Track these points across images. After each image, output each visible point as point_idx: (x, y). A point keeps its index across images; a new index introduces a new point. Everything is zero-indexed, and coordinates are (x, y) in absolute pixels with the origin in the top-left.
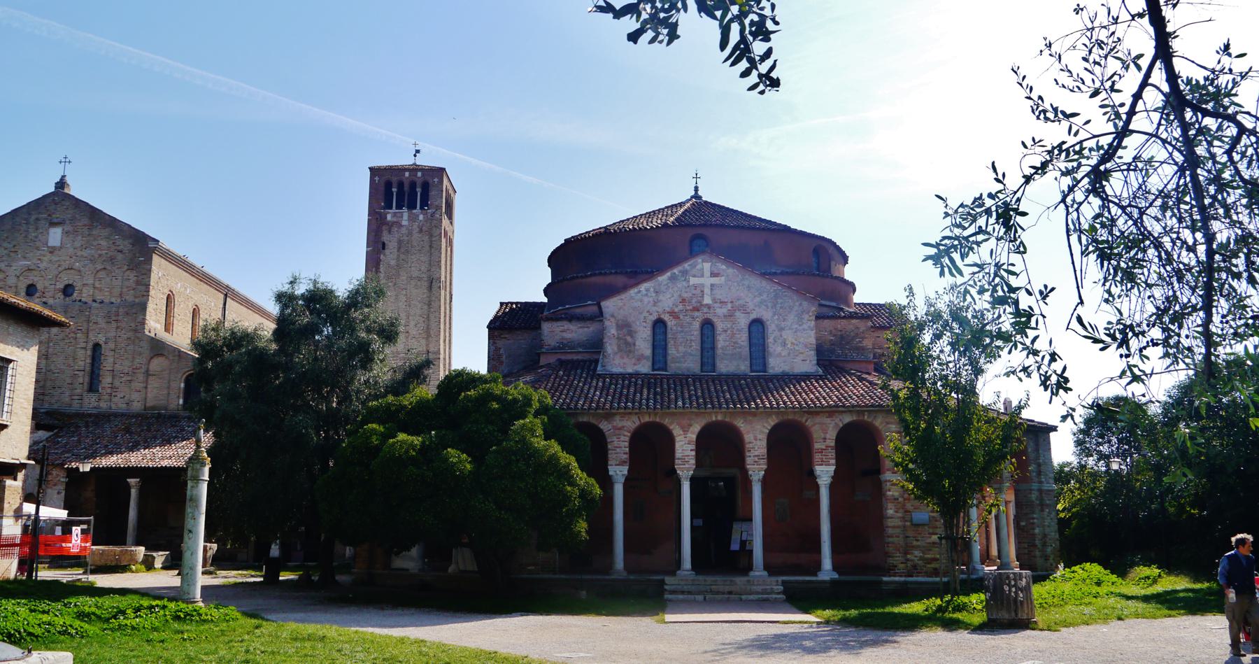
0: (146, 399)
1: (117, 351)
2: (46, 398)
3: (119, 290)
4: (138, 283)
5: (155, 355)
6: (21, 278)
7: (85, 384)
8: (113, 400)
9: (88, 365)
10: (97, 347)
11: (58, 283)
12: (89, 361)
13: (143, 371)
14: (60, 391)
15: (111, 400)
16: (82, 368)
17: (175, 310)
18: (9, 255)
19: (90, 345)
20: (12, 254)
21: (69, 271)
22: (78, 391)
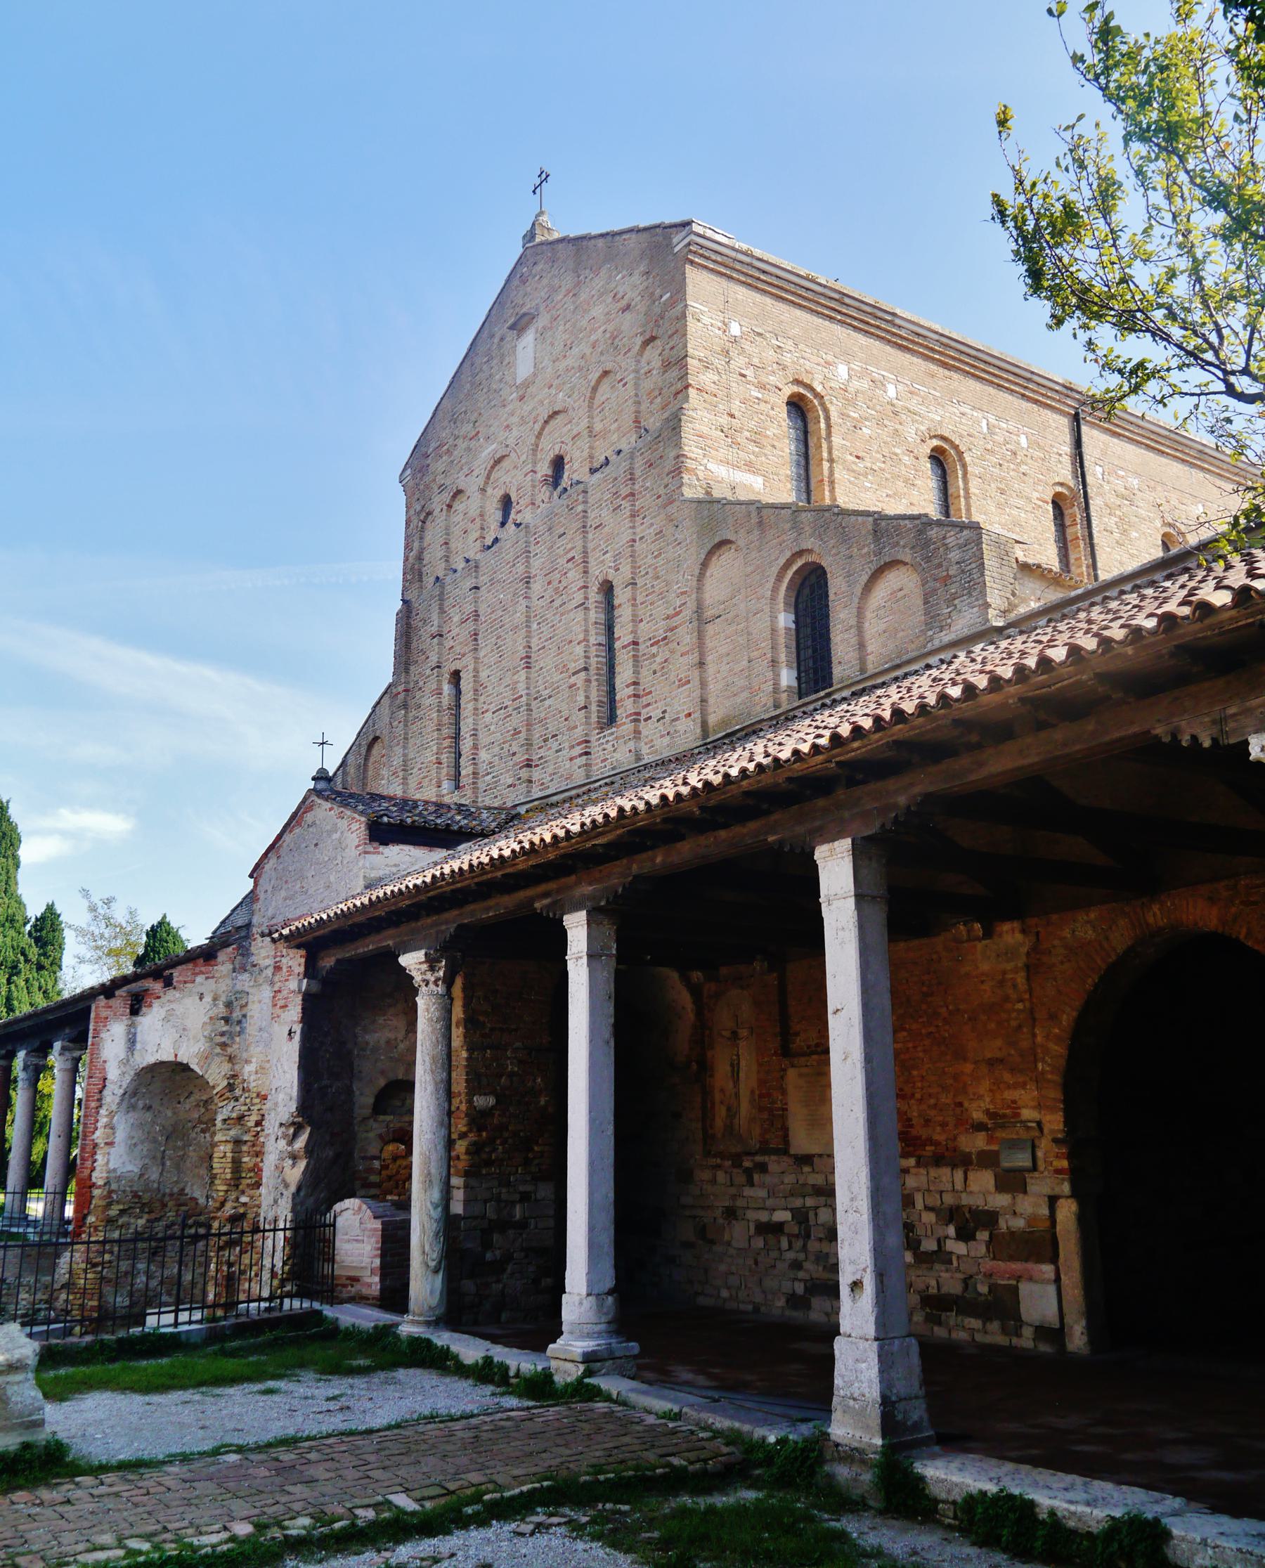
0: (703, 701)
1: (640, 582)
2: (536, 774)
3: (633, 409)
4: (667, 366)
5: (710, 553)
6: (489, 491)
7: (594, 708)
8: (644, 732)
9: (593, 651)
10: (608, 589)
11: (538, 468)
12: (597, 637)
13: (687, 613)
14: (555, 746)
15: (637, 732)
16: (581, 664)
17: (836, 440)
18: (469, 449)
19: (594, 596)
20: (473, 442)
21: (552, 423)
22: (579, 733)
